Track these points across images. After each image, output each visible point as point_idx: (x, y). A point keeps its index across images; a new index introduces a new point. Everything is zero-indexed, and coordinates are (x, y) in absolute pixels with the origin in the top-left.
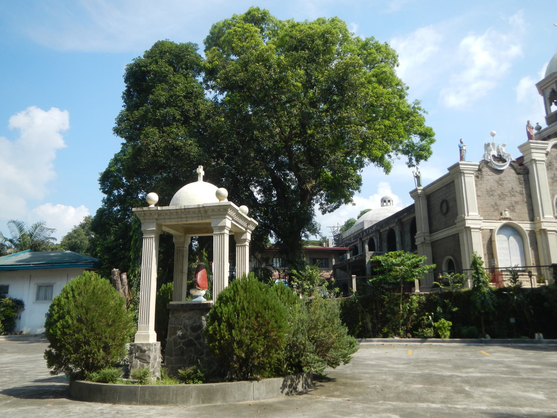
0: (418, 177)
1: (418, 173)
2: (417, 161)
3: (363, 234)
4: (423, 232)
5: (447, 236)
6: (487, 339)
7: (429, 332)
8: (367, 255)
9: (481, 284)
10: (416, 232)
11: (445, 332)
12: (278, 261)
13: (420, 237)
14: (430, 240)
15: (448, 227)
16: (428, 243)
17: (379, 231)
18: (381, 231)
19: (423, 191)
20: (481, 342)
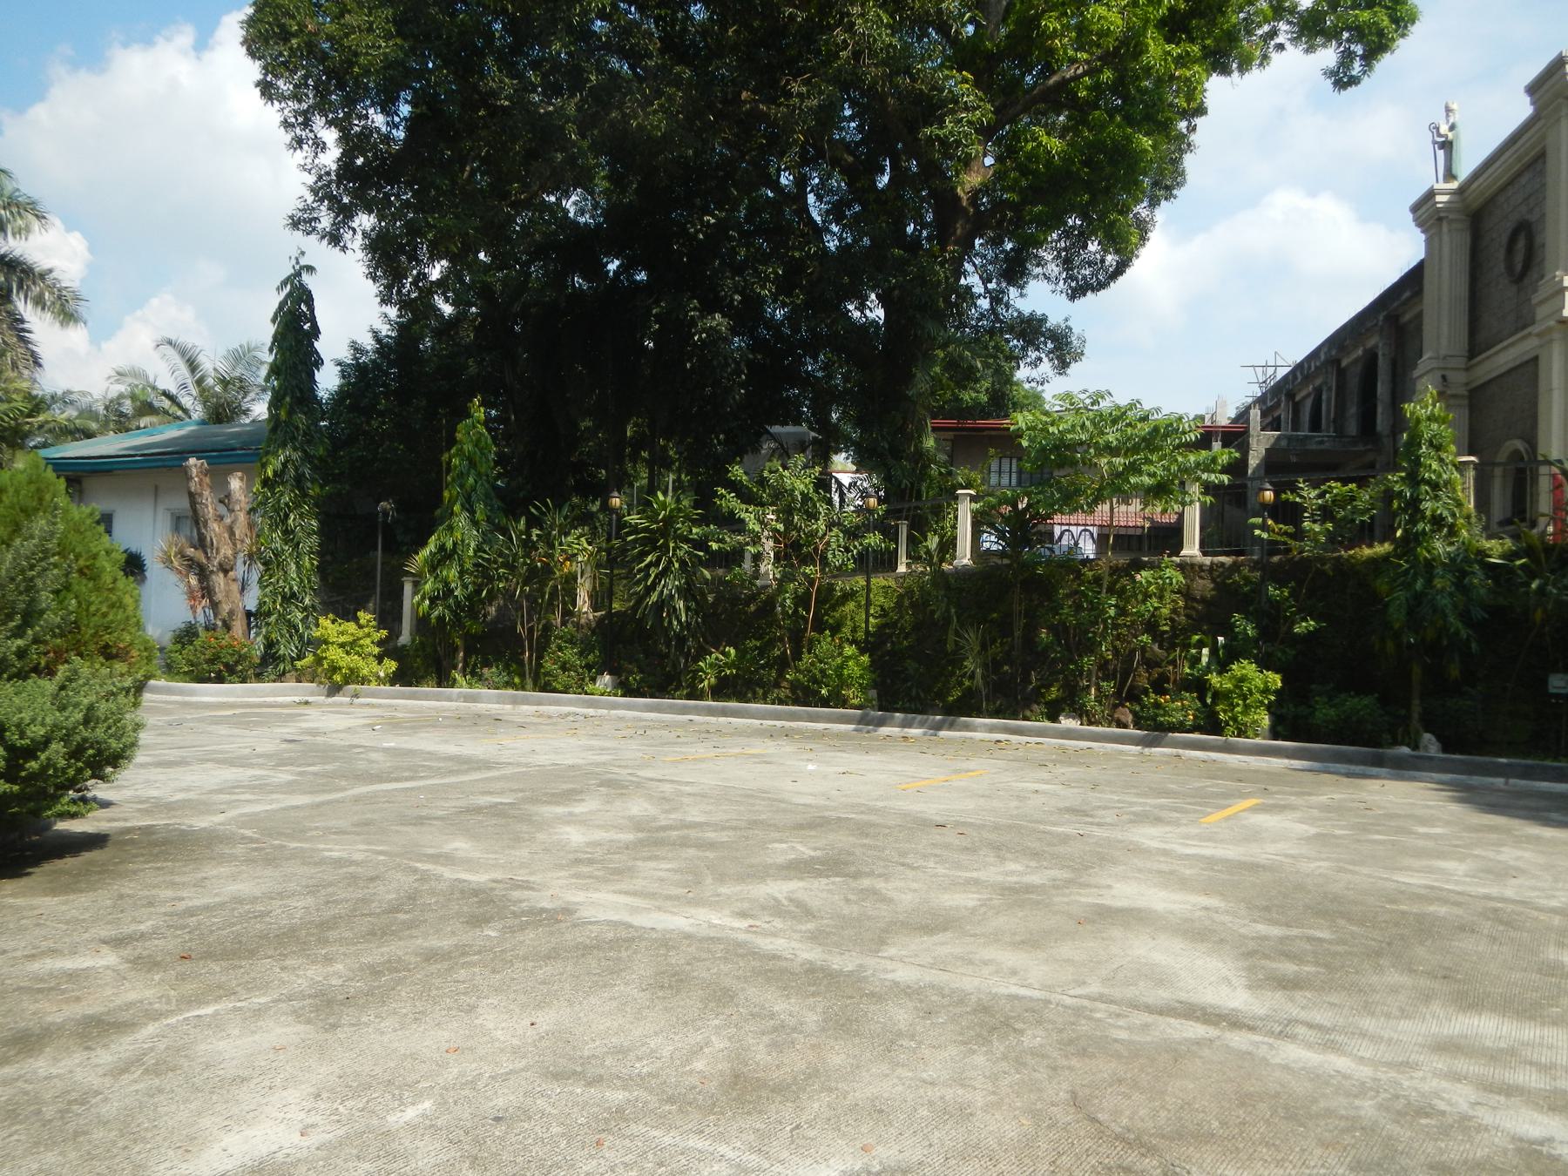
0: (1447, 146)
1: (1444, 129)
2: (1370, 57)
3: (1295, 378)
4: (1443, 352)
5: (1518, 362)
6: (1421, 753)
7: (1182, 707)
8: (1253, 442)
9: (1420, 526)
10: (1421, 357)
11: (1247, 707)
12: (1006, 467)
13: (1428, 372)
14: (1467, 384)
15: (1524, 327)
16: (1454, 396)
17: (1338, 361)
18: (1344, 363)
19: (1456, 198)
20: (1379, 762)
